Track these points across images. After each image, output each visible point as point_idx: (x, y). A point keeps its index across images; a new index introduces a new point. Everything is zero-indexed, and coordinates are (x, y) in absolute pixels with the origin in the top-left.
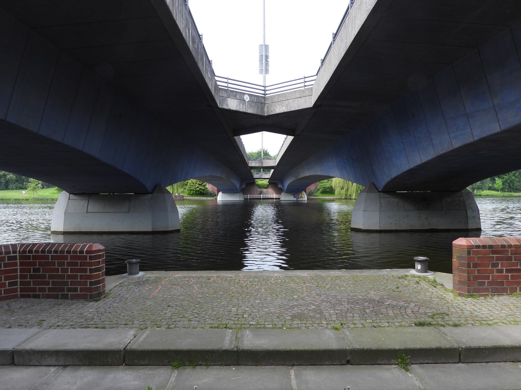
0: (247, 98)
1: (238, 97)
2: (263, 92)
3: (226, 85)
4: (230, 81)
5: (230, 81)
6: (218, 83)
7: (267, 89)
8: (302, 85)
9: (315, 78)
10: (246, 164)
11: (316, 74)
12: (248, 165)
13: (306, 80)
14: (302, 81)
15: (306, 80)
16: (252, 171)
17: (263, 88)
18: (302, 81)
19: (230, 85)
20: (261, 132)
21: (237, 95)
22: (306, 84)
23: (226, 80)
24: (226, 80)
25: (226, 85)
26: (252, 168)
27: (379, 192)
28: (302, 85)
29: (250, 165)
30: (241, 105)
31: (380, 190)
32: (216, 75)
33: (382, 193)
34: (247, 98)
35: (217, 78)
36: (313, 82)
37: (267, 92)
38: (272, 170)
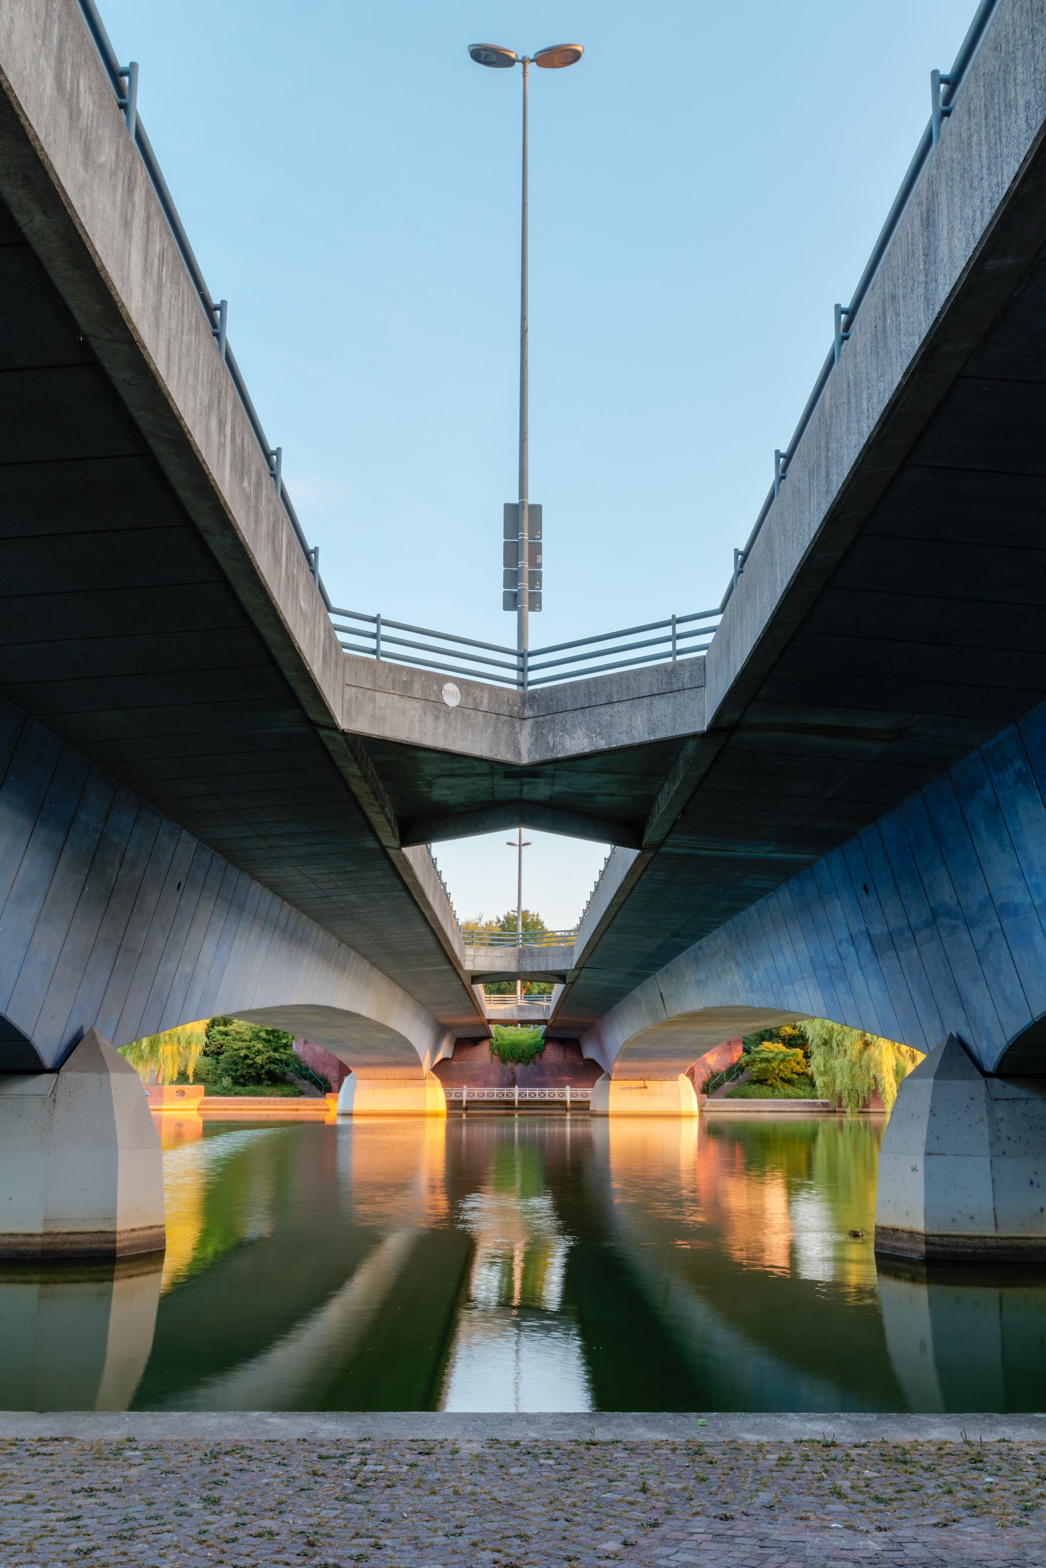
0: (452, 695)
1: (417, 690)
2: (513, 675)
3: (372, 643)
4: (385, 631)
5: (385, 631)
6: (342, 637)
7: (532, 661)
8: (667, 647)
9: (716, 620)
10: (451, 961)
11: (717, 605)
12: (461, 967)
13: (681, 628)
14: (667, 631)
15: (681, 628)
16: (479, 989)
17: (513, 660)
18: (667, 631)
19: (385, 647)
20: (511, 834)
21: (418, 684)
22: (681, 644)
23: (372, 628)
24: (372, 628)
25: (372, 643)
26: (477, 977)
27: (986, 1075)
28: (667, 647)
29: (468, 966)
30: (429, 720)
31: (990, 1066)
32: (334, 604)
33: (996, 1082)
34: (452, 695)
35: (335, 619)
36: (708, 639)
37: (532, 676)
38: (558, 989)
